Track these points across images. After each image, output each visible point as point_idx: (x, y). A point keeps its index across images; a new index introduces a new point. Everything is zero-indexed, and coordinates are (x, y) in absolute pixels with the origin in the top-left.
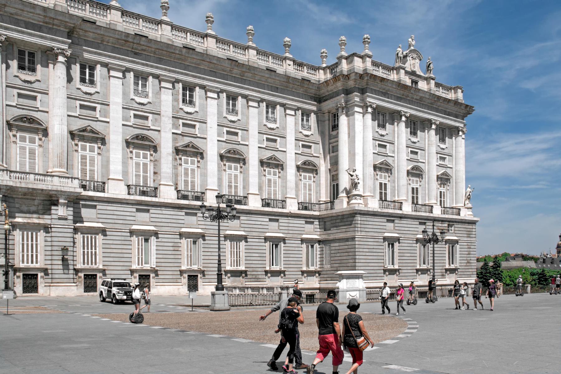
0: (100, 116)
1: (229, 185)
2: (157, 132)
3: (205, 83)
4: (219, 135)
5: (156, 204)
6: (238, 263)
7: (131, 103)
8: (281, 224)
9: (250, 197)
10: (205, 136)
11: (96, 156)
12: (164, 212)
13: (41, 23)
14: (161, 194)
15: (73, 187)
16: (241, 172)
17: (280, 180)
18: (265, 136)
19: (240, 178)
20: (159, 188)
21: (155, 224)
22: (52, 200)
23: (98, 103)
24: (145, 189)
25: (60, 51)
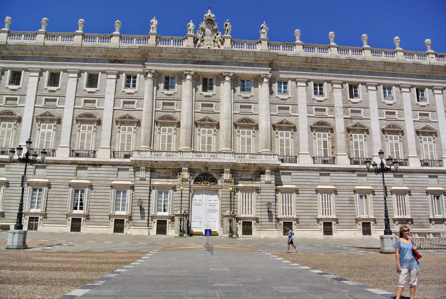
0: (292, 113)
1: (391, 152)
2: (333, 119)
3: (365, 80)
4: (380, 115)
5: (335, 169)
6: (405, 213)
7: (312, 102)
8: (440, 180)
9: (410, 159)
10: (369, 118)
11: (290, 139)
12: (341, 175)
13: (253, 62)
14: (338, 162)
15: (274, 161)
16: (400, 141)
17: (435, 144)
18: (418, 112)
19: (400, 145)
20: (336, 158)
21: (334, 184)
22: (261, 170)
23: (290, 105)
24: (326, 159)
25: (264, 76)
